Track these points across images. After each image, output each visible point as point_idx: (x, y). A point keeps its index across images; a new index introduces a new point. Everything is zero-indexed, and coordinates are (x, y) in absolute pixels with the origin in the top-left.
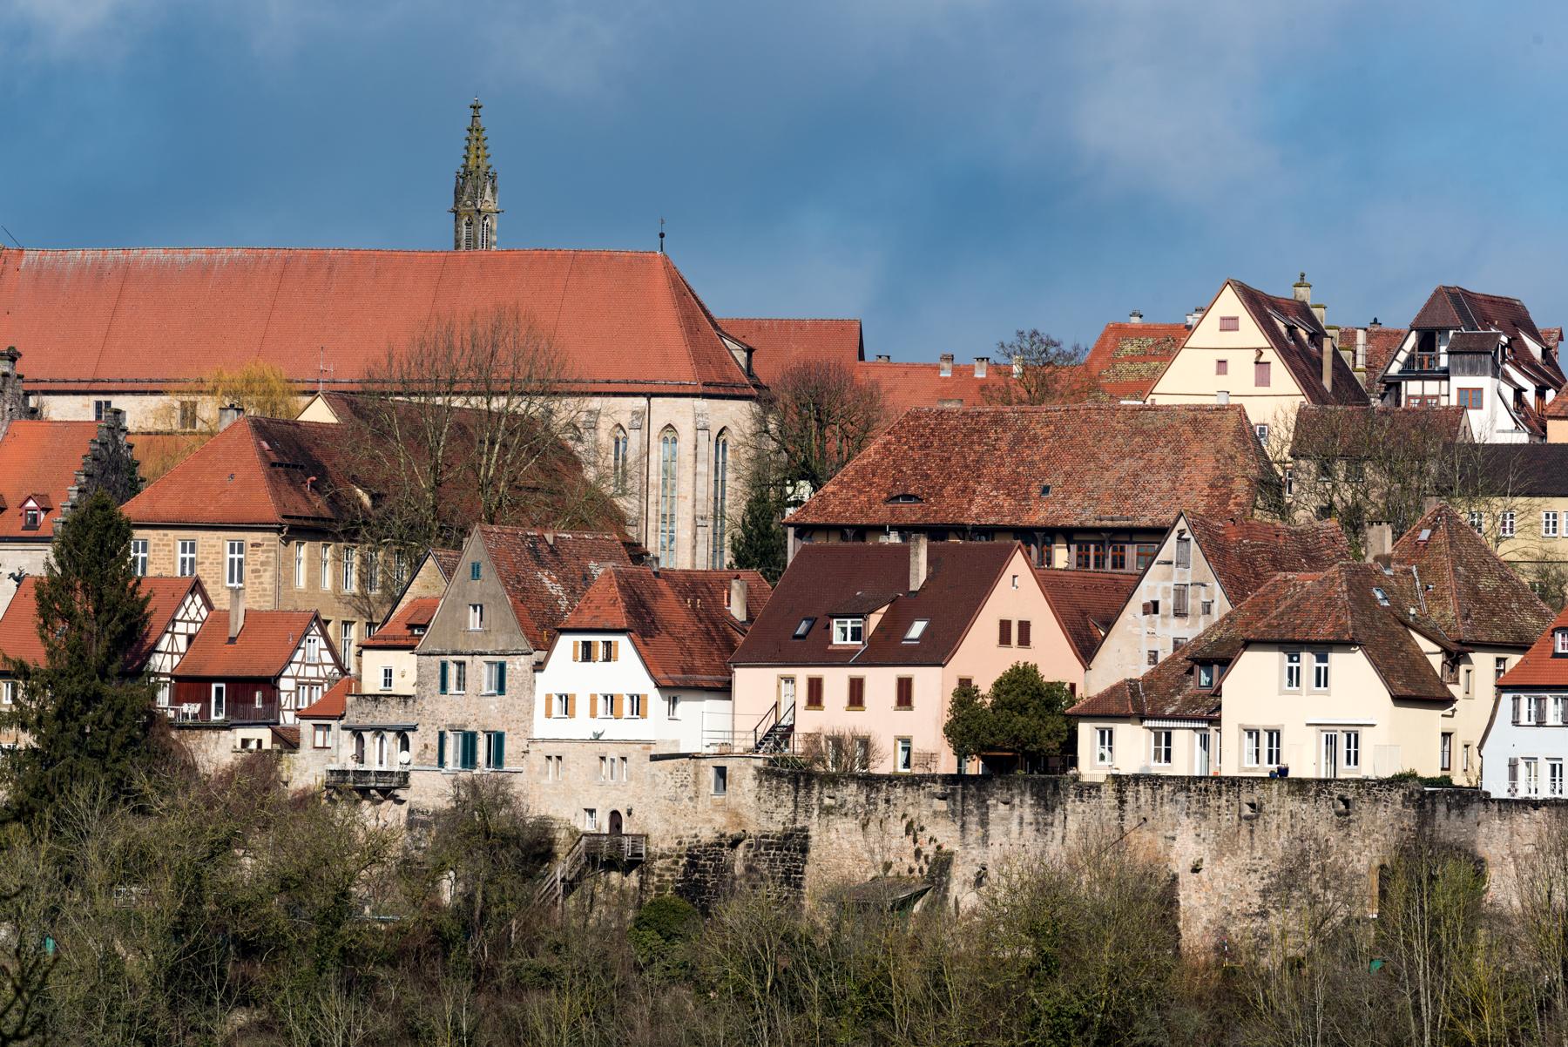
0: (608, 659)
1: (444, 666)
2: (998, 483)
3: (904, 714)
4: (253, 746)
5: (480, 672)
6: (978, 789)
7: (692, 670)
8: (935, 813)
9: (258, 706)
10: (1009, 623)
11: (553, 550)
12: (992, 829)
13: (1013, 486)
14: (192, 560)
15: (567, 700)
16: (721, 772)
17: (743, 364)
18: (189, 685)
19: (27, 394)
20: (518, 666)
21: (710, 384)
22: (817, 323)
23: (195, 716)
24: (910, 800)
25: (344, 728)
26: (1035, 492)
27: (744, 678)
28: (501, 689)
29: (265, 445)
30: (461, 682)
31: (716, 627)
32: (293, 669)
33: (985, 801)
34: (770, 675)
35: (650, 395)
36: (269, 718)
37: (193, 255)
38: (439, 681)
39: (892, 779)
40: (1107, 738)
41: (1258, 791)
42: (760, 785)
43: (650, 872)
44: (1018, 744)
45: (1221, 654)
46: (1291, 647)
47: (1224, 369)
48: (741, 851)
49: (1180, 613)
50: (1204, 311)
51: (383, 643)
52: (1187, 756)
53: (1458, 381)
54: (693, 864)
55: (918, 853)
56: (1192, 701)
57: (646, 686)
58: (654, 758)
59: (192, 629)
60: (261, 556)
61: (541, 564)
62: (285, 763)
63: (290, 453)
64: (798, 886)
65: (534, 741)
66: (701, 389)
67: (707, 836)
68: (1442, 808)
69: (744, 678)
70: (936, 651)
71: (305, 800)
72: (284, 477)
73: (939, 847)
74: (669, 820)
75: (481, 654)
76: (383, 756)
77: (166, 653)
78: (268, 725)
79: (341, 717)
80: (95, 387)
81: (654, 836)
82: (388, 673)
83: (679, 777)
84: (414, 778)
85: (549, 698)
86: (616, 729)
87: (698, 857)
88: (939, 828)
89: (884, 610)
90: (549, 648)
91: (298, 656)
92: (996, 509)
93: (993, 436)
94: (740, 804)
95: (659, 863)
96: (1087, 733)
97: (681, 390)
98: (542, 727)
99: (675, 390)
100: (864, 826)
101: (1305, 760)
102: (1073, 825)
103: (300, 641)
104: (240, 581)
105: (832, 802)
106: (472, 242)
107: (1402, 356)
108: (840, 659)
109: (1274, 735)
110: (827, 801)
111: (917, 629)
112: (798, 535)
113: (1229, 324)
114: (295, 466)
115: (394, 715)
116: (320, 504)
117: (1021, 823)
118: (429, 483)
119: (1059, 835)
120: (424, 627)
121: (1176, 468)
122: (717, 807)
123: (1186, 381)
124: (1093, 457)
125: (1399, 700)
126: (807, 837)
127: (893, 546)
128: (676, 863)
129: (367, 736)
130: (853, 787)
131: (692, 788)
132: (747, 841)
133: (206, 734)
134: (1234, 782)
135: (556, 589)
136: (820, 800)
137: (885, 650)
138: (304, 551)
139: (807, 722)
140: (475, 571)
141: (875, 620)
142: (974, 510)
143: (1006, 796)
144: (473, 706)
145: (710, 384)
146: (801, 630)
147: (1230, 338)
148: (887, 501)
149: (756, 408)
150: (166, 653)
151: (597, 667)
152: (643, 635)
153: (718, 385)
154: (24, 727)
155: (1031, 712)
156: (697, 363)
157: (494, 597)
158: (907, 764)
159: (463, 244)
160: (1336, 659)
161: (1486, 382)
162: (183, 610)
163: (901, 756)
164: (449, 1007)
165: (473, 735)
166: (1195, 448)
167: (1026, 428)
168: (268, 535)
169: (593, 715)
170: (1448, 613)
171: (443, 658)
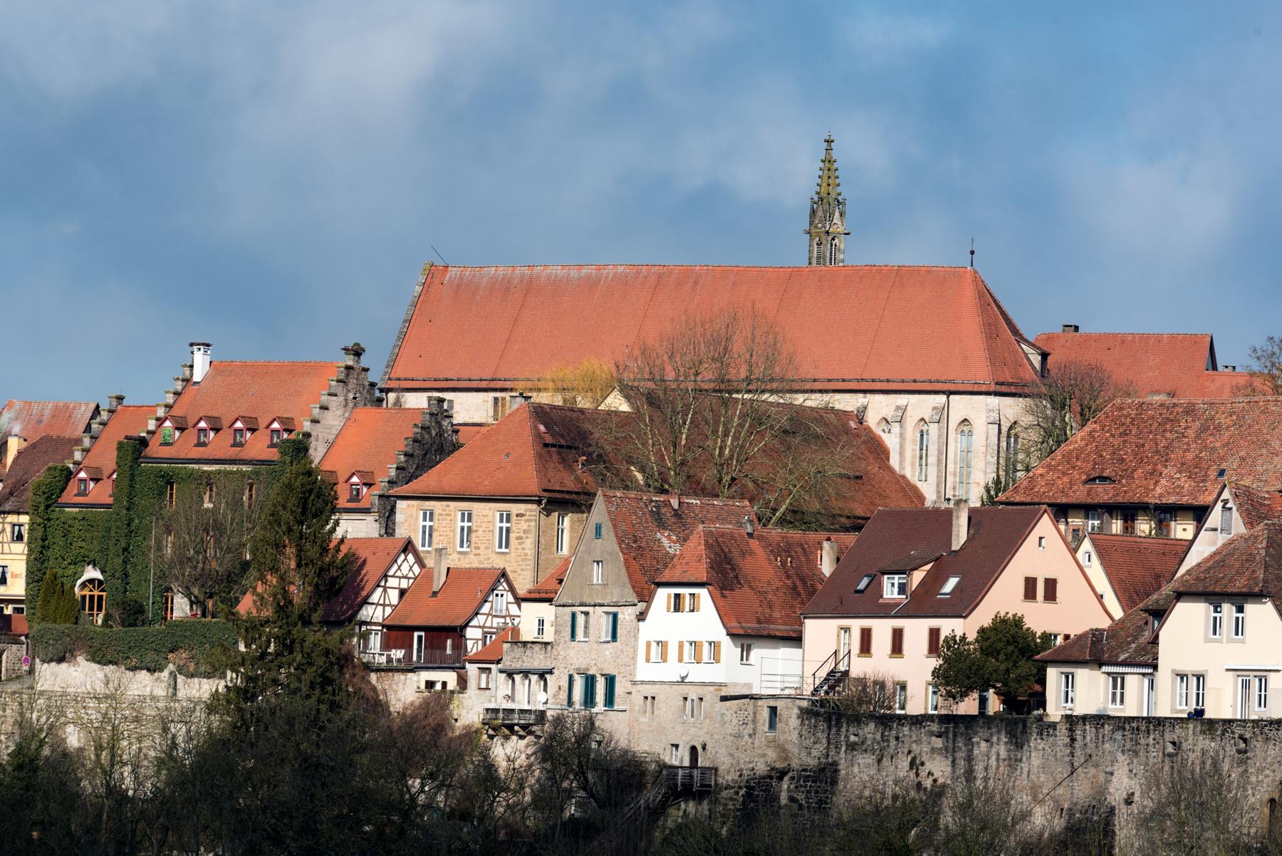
0: (693, 611)
1: (574, 616)
4: (438, 687)
5: (600, 619)
6: (966, 728)
7: (769, 620)
8: (933, 750)
10: (1035, 580)
11: (677, 514)
13: (1195, 470)
14: (469, 528)
16: (773, 710)
17: (1037, 366)
18: (396, 633)
20: (627, 615)
21: (1002, 384)
22: (1173, 337)
23: (399, 660)
24: (914, 738)
25: (501, 671)
26: (1213, 474)
29: (542, 428)
31: (803, 581)
32: (480, 620)
33: (970, 739)
34: (833, 624)
35: (949, 393)
37: (585, 271)
38: (569, 629)
41: (1178, 730)
42: (802, 724)
46: (1214, 597)
51: (537, 596)
57: (717, 631)
58: (724, 699)
59: (404, 584)
60: (524, 526)
61: (661, 524)
62: (456, 702)
65: (634, 683)
66: (993, 388)
67: (761, 768)
71: (470, 735)
72: (555, 457)
73: (935, 781)
74: (735, 754)
75: (601, 605)
77: (378, 604)
78: (453, 669)
79: (498, 662)
80: (493, 385)
81: (722, 768)
83: (742, 714)
85: (648, 645)
87: (753, 788)
88: (936, 763)
89: (928, 567)
91: (486, 608)
92: (1178, 490)
93: (1183, 424)
94: (786, 741)
95: (725, 794)
97: (976, 389)
98: (645, 671)
99: (970, 389)
100: (879, 761)
101: (1222, 705)
102: (1036, 760)
103: (488, 596)
104: (507, 547)
105: (856, 739)
108: (885, 611)
110: (852, 738)
111: (952, 583)
114: (569, 447)
115: (537, 660)
117: (998, 760)
119: (1025, 772)
124: (1266, 443)
126: (837, 771)
128: (737, 793)
130: (872, 726)
131: (751, 726)
132: (790, 774)
136: (847, 737)
141: (918, 576)
142: (1159, 490)
143: (986, 735)
145: (1002, 384)
146: (861, 586)
148: (1086, 482)
150: (378, 604)
151: (684, 616)
152: (723, 588)
153: (1010, 384)
155: (1001, 657)
156: (993, 364)
157: (611, 554)
159: (814, 261)
162: (395, 567)
167: (1212, 418)
168: (529, 506)
171: (574, 609)
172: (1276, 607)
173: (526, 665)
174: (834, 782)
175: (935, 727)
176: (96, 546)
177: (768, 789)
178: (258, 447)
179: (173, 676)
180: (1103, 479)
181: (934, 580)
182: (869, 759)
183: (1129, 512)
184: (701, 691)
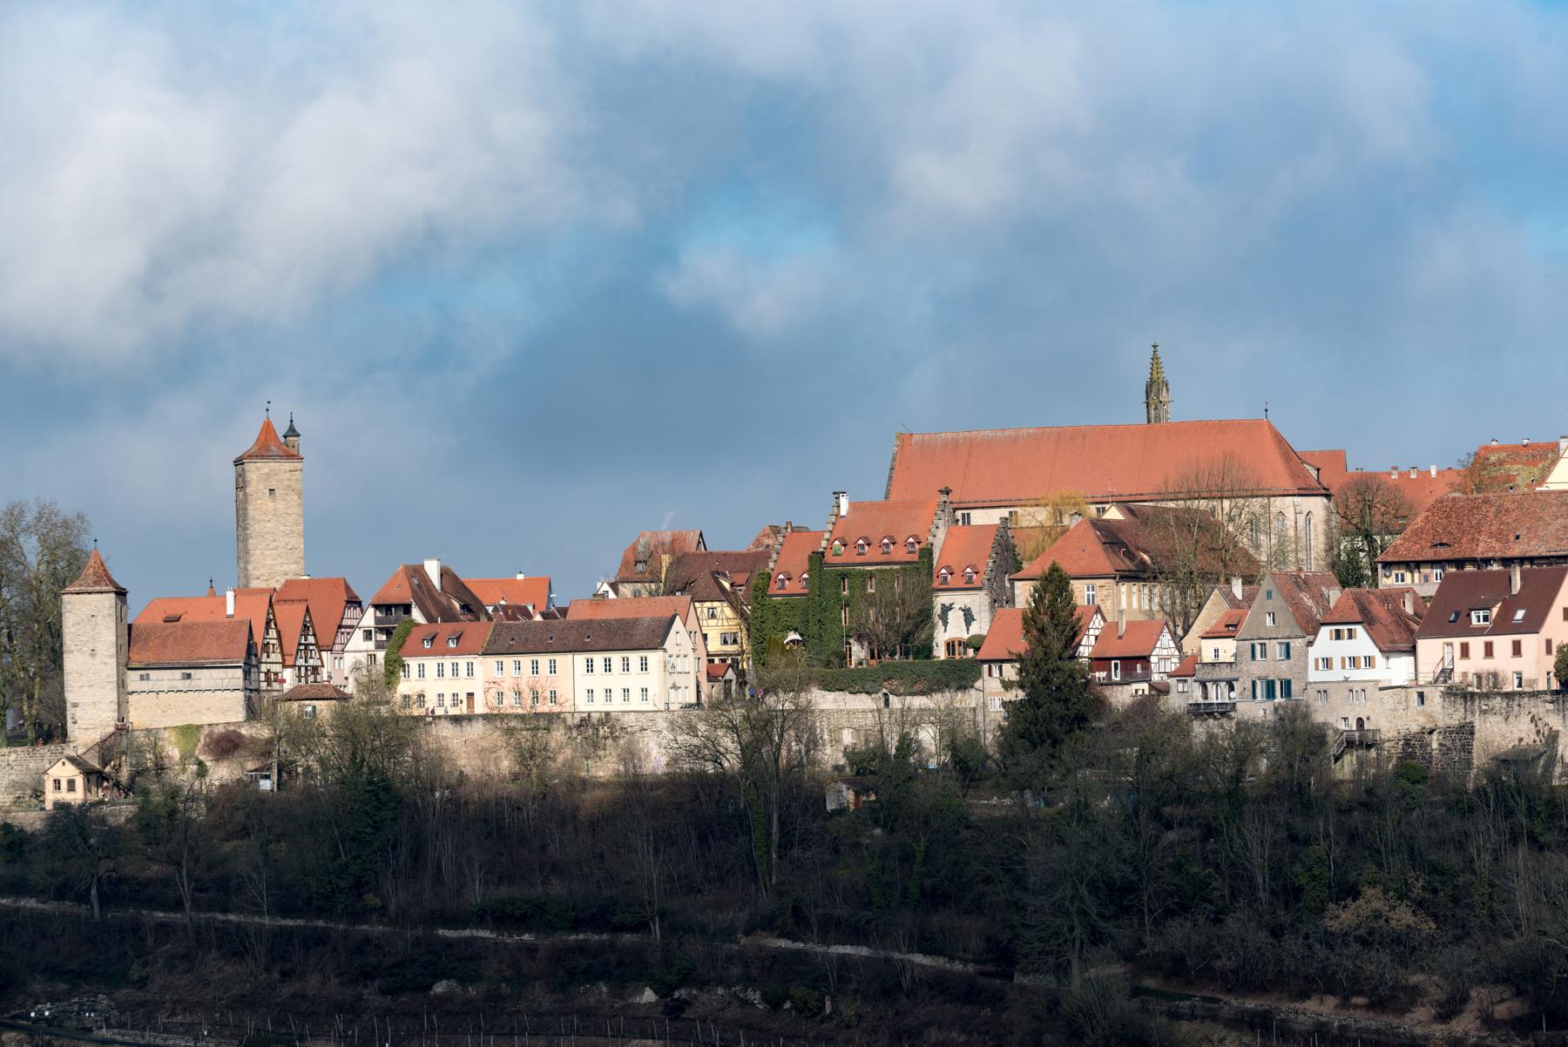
0: (1350, 637)
2: (1491, 535)
3: (1517, 660)
5: (1275, 648)
7: (1394, 642)
13: (1499, 536)
15: (1328, 663)
16: (1421, 695)
18: (1100, 661)
20: (1297, 644)
22: (1321, 453)
26: (1512, 538)
27: (1423, 645)
28: (1288, 656)
30: (1264, 654)
34: (1440, 642)
36: (1146, 678)
39: (1520, 694)
54: (1407, 743)
55: (1538, 732)
57: (1373, 650)
61: (1301, 590)
63: (1111, 537)
67: (1415, 728)
69: (1423, 645)
70: (1533, 624)
74: (1391, 721)
76: (1218, 695)
81: (1384, 730)
82: (1216, 651)
84: (1239, 706)
90: (1316, 634)
92: (1492, 549)
98: (1313, 675)
111: (1520, 614)
115: (1226, 673)
118: (1173, 551)
124: (1541, 519)
130: (1499, 699)
135: (1310, 603)
137: (1503, 626)
138: (1124, 588)
139: (1461, 666)
140: (1269, 595)
141: (1495, 610)
144: (1273, 665)
154: (1022, 687)
158: (1520, 685)
163: (1516, 682)
164: (1321, 824)
174: (1472, 733)
175: (1548, 698)
176: (797, 619)
178: (899, 553)
180: (1442, 544)
181: (1506, 613)
182: (1499, 718)
183: (1460, 563)
184: (1363, 686)
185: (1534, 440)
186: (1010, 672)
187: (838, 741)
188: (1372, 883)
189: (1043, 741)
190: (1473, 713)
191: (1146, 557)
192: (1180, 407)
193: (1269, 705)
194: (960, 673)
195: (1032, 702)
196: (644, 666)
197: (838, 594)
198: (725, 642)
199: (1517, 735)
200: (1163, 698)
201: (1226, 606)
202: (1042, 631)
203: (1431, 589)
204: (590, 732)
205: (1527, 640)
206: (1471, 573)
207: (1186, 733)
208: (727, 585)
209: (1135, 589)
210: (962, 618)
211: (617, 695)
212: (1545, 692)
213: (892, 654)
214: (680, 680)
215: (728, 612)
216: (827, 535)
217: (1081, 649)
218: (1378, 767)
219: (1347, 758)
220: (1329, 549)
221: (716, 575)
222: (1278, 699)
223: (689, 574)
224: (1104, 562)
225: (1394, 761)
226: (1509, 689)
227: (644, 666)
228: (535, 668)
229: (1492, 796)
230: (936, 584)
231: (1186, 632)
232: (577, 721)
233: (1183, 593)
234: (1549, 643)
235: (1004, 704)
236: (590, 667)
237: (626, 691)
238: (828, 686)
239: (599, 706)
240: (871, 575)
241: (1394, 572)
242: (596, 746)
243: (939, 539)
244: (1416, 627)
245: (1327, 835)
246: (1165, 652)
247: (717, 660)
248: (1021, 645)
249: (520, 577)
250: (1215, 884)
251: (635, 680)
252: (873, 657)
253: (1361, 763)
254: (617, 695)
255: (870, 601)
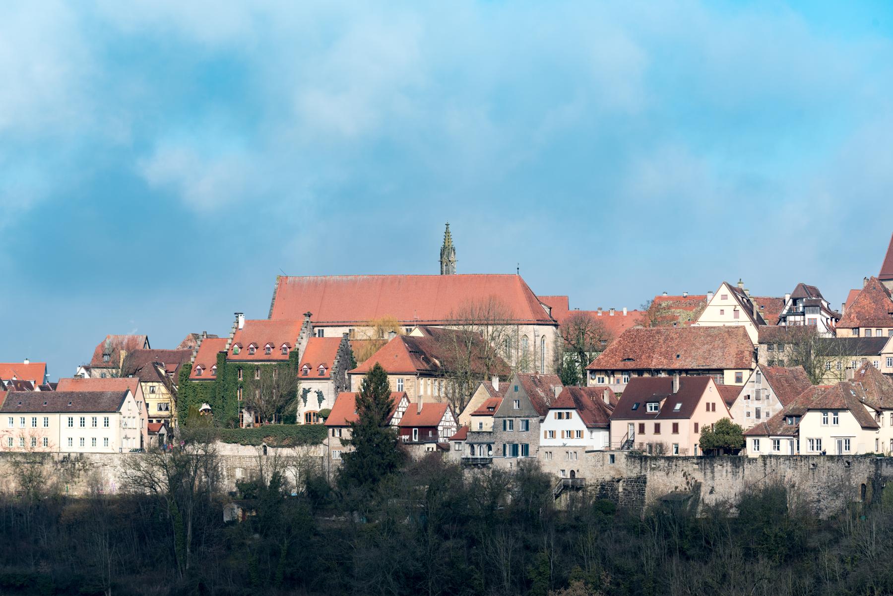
0: (568, 418)
1: (505, 421)
3: (675, 435)
5: (519, 423)
9: (430, 436)
12: (716, 474)
13: (666, 355)
15: (552, 434)
18: (405, 429)
19: (314, 327)
20: (533, 421)
22: (552, 297)
26: (674, 357)
27: (615, 424)
28: (527, 429)
30: (511, 427)
34: (625, 423)
35: (518, 325)
36: (435, 440)
37: (349, 278)
39: (677, 458)
40: (757, 443)
41: (816, 460)
43: (586, 491)
44: (722, 446)
45: (796, 413)
46: (825, 410)
47: (720, 312)
48: (621, 483)
49: (758, 399)
50: (714, 293)
52: (785, 448)
53: (807, 316)
54: (603, 487)
55: (688, 483)
56: (786, 429)
57: (582, 426)
58: (587, 452)
59: (404, 410)
60: (410, 384)
61: (537, 386)
63: (415, 348)
64: (643, 495)
67: (608, 478)
68: (884, 464)
69: (615, 424)
70: (686, 413)
74: (592, 473)
76: (481, 453)
81: (588, 479)
82: (481, 424)
84: (494, 460)
85: (546, 432)
86: (575, 442)
90: (545, 414)
95: (589, 488)
96: (749, 441)
98: (543, 442)
102: (747, 472)
106: (448, 272)
107: (787, 308)
108: (651, 417)
109: (819, 441)
111: (678, 406)
112: (591, 373)
113: (724, 297)
115: (486, 439)
116: (426, 366)
120: (494, 408)
121: (723, 348)
122: (611, 468)
123: (710, 318)
125: (864, 428)
127: (664, 378)
129: (475, 446)
130: (663, 461)
133: (414, 446)
134: (806, 457)
137: (667, 413)
138: (422, 381)
139: (639, 439)
140: (516, 389)
141: (662, 403)
142: (653, 363)
144: (518, 435)
147: (725, 302)
149: (554, 328)
158: (677, 452)
160: (841, 415)
161: (817, 316)
163: (674, 450)
164: (546, 538)
165: (517, 445)
166: (729, 341)
169: (563, 437)
170: (875, 398)
172: (853, 414)
173: (479, 441)
174: (645, 483)
175: (695, 461)
177: (612, 486)
178: (277, 354)
179: (265, 446)
180: (629, 359)
181: (669, 406)
182: (662, 473)
183: (640, 372)
184: (575, 449)
185: (691, 294)
186: (346, 434)
187: (233, 476)
188: (578, 578)
189: (367, 480)
190: (646, 469)
191: (437, 362)
192: (461, 266)
193: (514, 461)
194: (314, 434)
195: (359, 454)
196: (106, 423)
197: (236, 380)
198: (161, 409)
199: (674, 485)
200: (445, 454)
201: (488, 396)
202: (368, 407)
203: (621, 388)
204: (70, 465)
205: (683, 424)
206: (647, 379)
207: (461, 476)
208: (163, 372)
209: (429, 382)
210: (316, 398)
211: (88, 441)
212: (693, 457)
213: (270, 420)
214: (130, 433)
215: (163, 389)
216: (230, 341)
217: (393, 420)
218: (584, 503)
219: (563, 496)
220: (556, 360)
221: (156, 365)
222: (520, 457)
223: (139, 364)
224: (409, 364)
225: (594, 499)
226: (669, 454)
227: (106, 423)
228: (35, 423)
229: (657, 524)
230: (300, 375)
231: (462, 411)
232: (61, 458)
233: (461, 385)
234: (696, 425)
235: (342, 455)
236: (71, 423)
237: (94, 439)
238: (227, 440)
239: (75, 449)
240: (258, 368)
241: (598, 376)
242: (73, 475)
243: (303, 346)
244: (611, 413)
245: (549, 546)
246: (447, 424)
247: (155, 421)
248: (354, 417)
249: (26, 362)
250: (476, 576)
251: (100, 432)
252: (257, 422)
253: (573, 500)
254: (88, 441)
255: (257, 385)
